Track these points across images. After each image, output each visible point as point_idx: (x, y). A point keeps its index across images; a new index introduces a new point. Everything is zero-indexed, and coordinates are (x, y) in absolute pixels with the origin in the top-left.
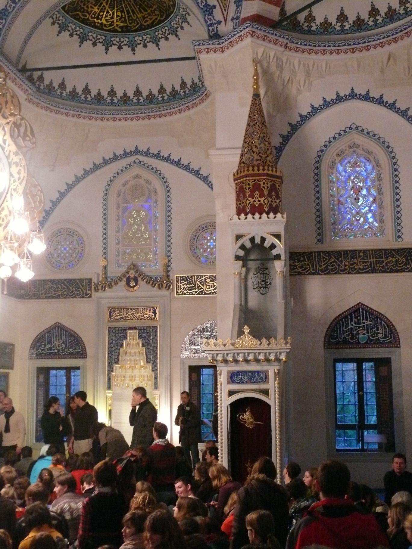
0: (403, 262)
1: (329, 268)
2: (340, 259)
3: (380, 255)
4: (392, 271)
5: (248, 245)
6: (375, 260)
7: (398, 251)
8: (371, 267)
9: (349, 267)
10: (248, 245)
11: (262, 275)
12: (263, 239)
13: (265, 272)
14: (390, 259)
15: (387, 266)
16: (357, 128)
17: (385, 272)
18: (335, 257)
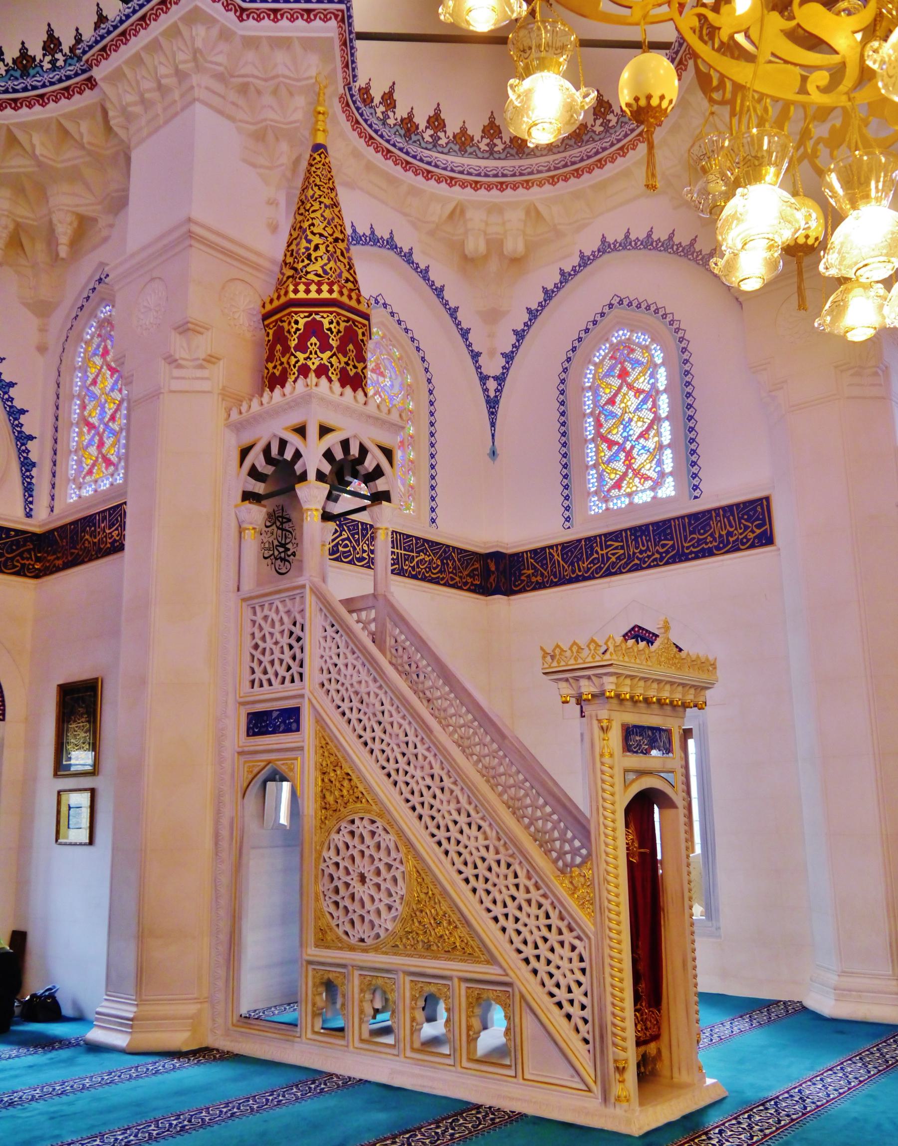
0: (438, 566)
1: (341, 549)
2: (356, 536)
3: (409, 546)
4: (424, 579)
5: (339, 455)
6: (403, 552)
7: (433, 544)
8: (398, 564)
9: (368, 555)
10: (339, 455)
11: (280, 532)
12: (363, 451)
13: (286, 526)
14: (422, 556)
15: (418, 567)
16: (385, 305)
17: (414, 577)
18: (349, 530)
